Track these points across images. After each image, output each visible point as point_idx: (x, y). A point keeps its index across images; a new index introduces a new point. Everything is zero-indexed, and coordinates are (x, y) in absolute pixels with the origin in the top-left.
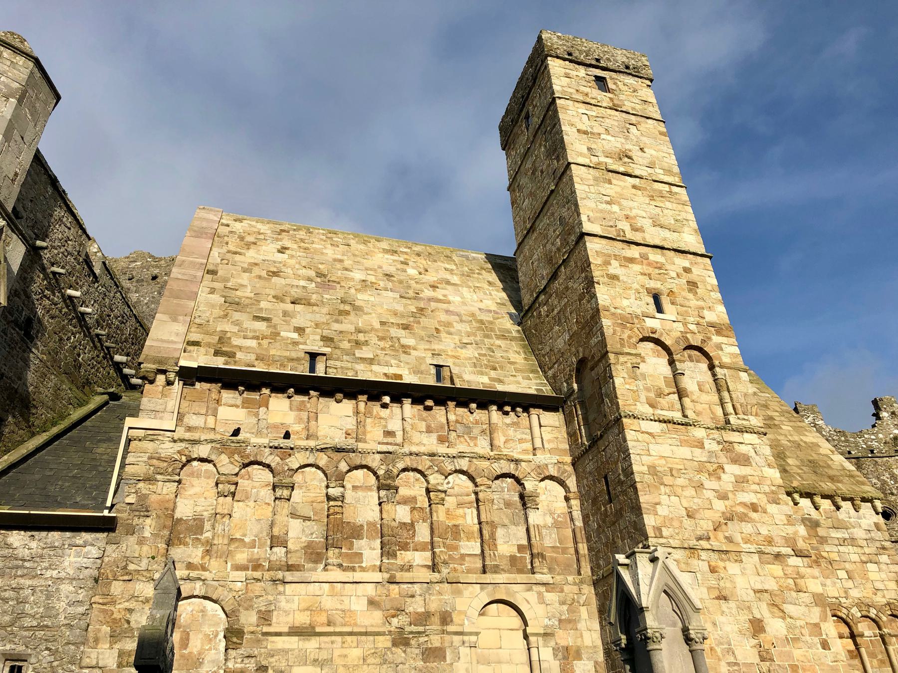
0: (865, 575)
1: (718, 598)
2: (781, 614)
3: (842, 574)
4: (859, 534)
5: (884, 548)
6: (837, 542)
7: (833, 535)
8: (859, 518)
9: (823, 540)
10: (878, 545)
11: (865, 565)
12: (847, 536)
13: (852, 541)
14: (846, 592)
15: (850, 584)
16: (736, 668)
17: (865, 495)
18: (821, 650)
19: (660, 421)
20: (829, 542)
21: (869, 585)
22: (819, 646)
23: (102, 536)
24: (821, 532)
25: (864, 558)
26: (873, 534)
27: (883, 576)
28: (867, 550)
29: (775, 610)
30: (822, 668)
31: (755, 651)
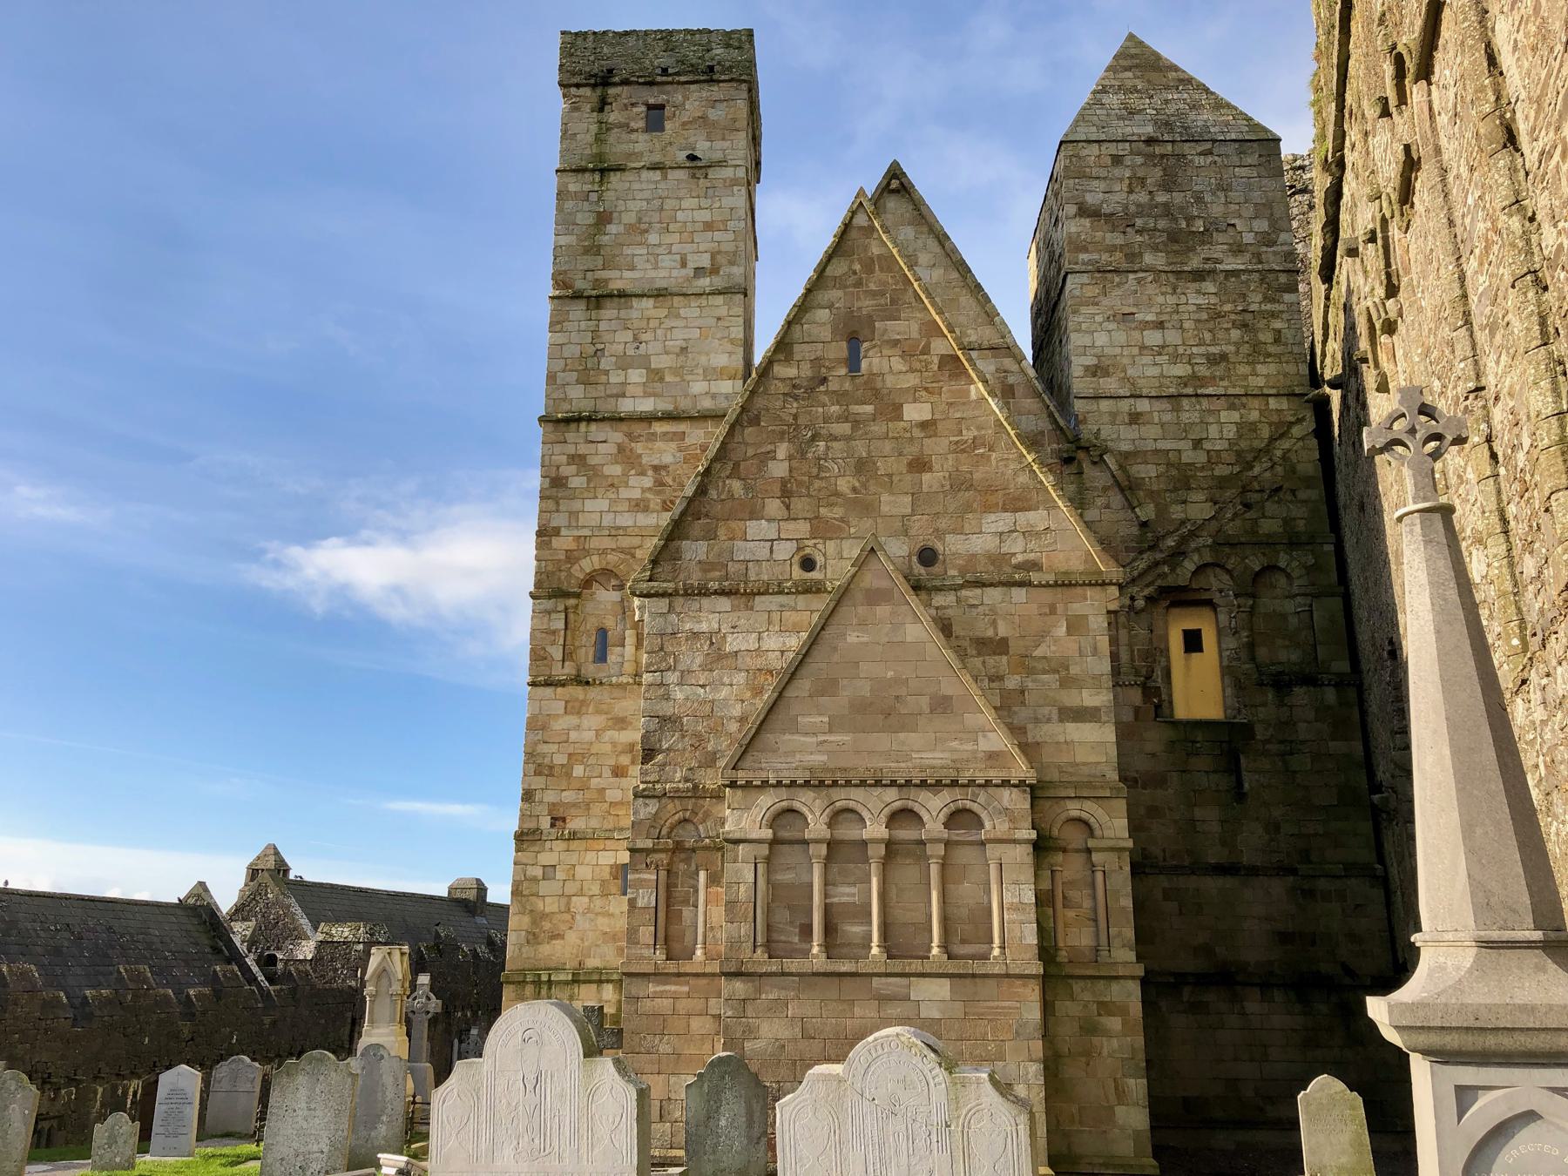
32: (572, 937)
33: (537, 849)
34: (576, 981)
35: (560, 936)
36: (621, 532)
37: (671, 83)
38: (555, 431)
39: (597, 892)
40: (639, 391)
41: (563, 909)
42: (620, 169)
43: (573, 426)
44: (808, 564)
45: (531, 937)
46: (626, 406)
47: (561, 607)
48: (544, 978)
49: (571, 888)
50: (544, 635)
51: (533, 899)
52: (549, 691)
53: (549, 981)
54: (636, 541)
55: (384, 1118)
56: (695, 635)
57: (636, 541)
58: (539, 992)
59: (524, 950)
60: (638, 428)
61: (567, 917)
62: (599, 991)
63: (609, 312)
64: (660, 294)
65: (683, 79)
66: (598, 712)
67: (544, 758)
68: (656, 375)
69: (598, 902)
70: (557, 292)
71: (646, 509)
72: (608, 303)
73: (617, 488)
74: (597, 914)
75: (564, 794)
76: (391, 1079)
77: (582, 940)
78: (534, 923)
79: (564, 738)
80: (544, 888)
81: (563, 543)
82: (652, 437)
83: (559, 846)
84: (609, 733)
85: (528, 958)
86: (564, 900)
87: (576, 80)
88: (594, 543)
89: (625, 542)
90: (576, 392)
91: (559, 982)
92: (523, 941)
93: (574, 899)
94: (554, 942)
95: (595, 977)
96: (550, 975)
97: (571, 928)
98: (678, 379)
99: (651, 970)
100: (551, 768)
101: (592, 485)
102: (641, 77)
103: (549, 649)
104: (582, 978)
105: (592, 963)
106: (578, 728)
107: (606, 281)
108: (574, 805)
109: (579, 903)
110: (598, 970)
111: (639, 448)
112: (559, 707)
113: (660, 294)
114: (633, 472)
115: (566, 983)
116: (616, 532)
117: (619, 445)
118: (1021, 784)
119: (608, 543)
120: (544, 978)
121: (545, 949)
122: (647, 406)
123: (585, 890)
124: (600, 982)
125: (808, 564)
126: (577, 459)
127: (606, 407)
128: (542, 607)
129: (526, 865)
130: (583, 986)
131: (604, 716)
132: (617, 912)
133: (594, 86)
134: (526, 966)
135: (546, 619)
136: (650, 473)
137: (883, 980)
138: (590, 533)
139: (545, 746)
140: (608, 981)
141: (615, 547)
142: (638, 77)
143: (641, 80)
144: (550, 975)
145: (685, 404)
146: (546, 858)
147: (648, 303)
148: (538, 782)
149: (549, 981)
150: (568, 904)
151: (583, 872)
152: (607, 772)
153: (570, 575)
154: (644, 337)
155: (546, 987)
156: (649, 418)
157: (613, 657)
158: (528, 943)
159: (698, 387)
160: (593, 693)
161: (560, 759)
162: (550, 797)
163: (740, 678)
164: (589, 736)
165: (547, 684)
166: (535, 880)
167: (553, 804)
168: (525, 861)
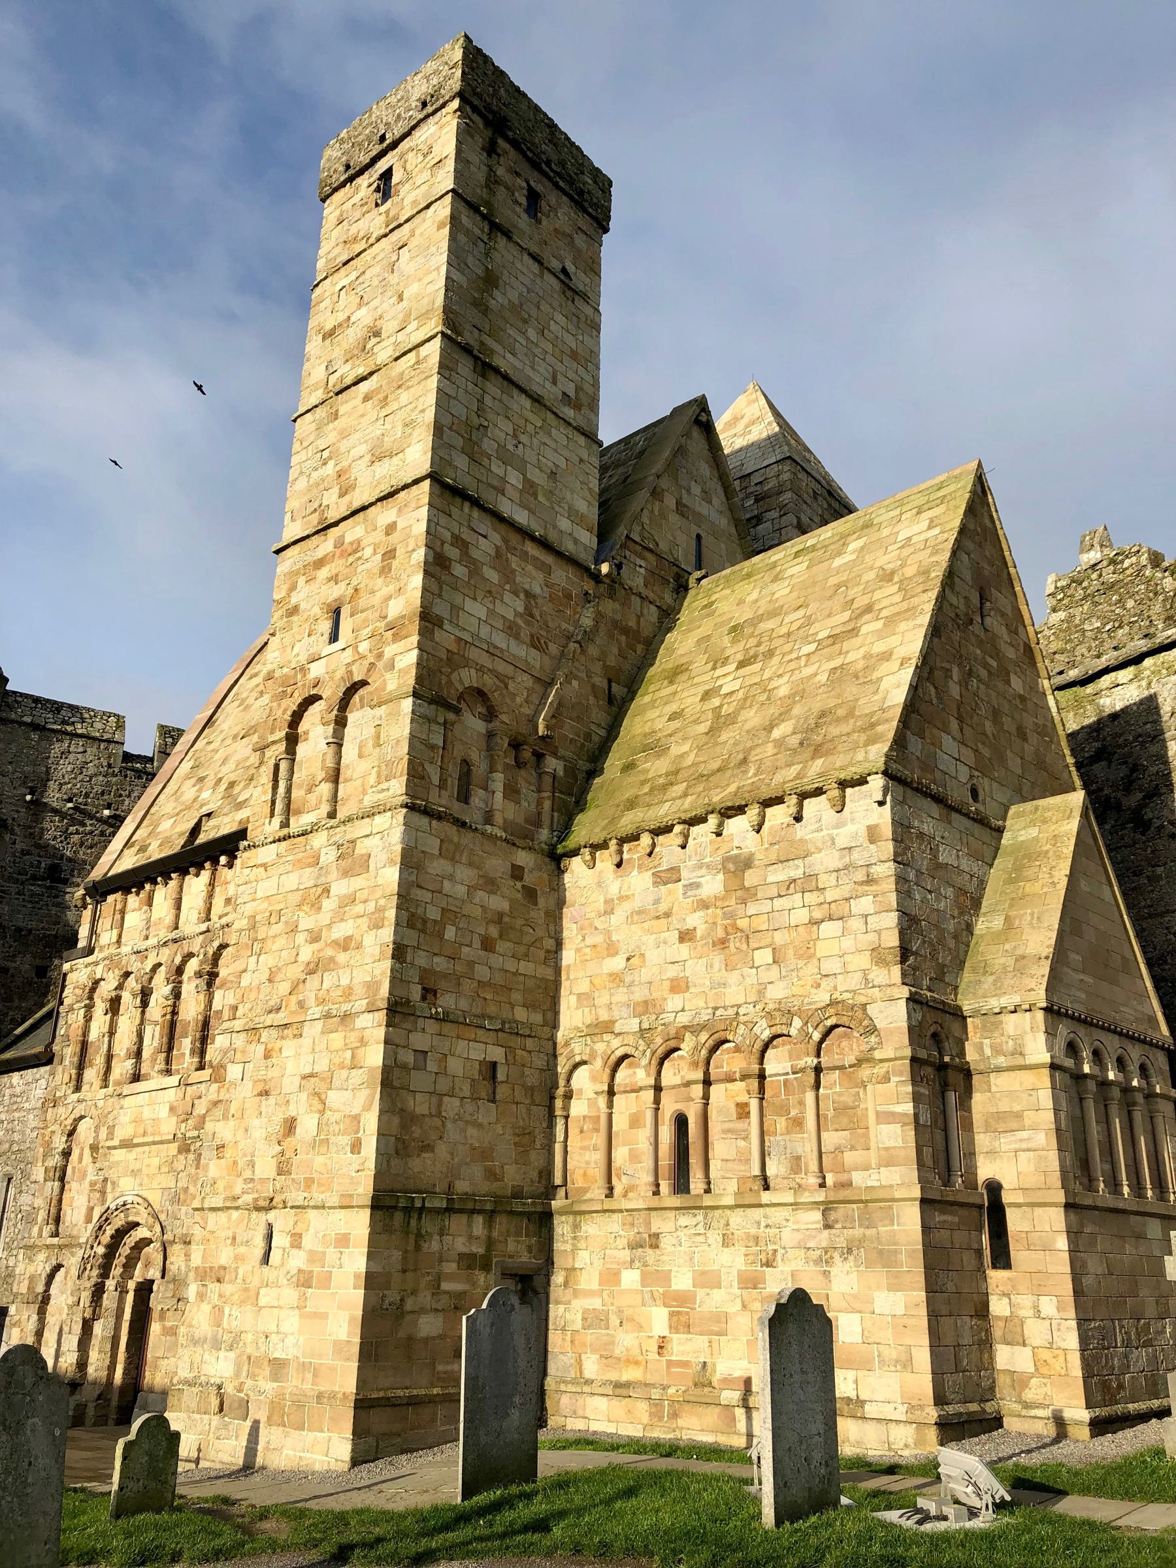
0: (807, 953)
1: (260, 1094)
2: (320, 1107)
3: (763, 957)
4: (825, 861)
5: (870, 881)
6: (774, 892)
7: (770, 879)
8: (838, 826)
9: (748, 895)
10: (860, 876)
11: (815, 927)
12: (798, 873)
13: (808, 883)
14: (759, 992)
15: (774, 973)
16: (250, 1185)
17: (842, 776)
18: (349, 1155)
19: (279, 840)
20: (759, 896)
21: (811, 969)
22: (348, 1149)
23: (43, 1069)
24: (751, 878)
25: (818, 915)
26: (855, 855)
27: (848, 943)
28: (830, 895)
29: (316, 1102)
30: (341, 1181)
31: (274, 1162)
32: (442, 1150)
33: (408, 1025)
34: (449, 1210)
35: (428, 1148)
36: (497, 653)
37: (550, 179)
38: (440, 496)
39: (467, 1093)
40: (516, 496)
41: (434, 1112)
42: (508, 235)
43: (458, 500)
44: (974, 793)
45: (400, 1146)
46: (506, 508)
47: (441, 720)
48: (418, 1204)
49: (443, 1085)
50: (423, 747)
51: (403, 1092)
52: (424, 821)
53: (423, 1208)
54: (510, 670)
55: (517, 1399)
56: (921, 835)
57: (510, 670)
58: (409, 1223)
59: (392, 1163)
60: (514, 539)
61: (437, 1122)
62: (470, 1225)
63: (493, 388)
64: (537, 400)
65: (562, 184)
66: (470, 864)
67: (417, 906)
68: (530, 488)
69: (469, 1107)
70: (449, 332)
71: (517, 637)
72: (492, 375)
73: (495, 598)
74: (467, 1122)
75: (436, 959)
76: (523, 1340)
77: (452, 1154)
78: (404, 1126)
79: (436, 887)
80: (419, 1081)
81: (445, 638)
82: (524, 556)
83: (432, 1026)
84: (480, 893)
85: (397, 1175)
86: (434, 1100)
87: (476, 102)
88: (474, 654)
89: (502, 667)
90: (461, 462)
91: (430, 1210)
92: (392, 1152)
93: (446, 1099)
94: (424, 1155)
95: (470, 1206)
96: (424, 1199)
97: (441, 1138)
98: (547, 504)
99: (939, 1198)
100: (425, 921)
101: (472, 582)
102: (531, 151)
103: (427, 765)
104: (456, 1206)
105: (462, 1186)
106: (451, 878)
107: (492, 352)
108: (446, 976)
109: (451, 1106)
110: (467, 1197)
111: (514, 562)
112: (432, 845)
113: (537, 400)
114: (507, 587)
115: (437, 1211)
116: (492, 652)
117: (497, 547)
118: (1168, 1050)
119: (484, 659)
120: (418, 1204)
121: (415, 1164)
122: (521, 517)
123: (457, 1090)
124: (473, 1212)
125: (974, 793)
126: (458, 541)
127: (488, 497)
128: (422, 710)
129: (397, 1046)
130: (454, 1217)
131: (476, 871)
132: (485, 1122)
133: (487, 123)
134: (397, 1186)
135: (426, 726)
136: (522, 596)
137: (1138, 1218)
138: (470, 640)
139: (419, 892)
140: (479, 1212)
141: (490, 667)
142: (528, 149)
143: (530, 154)
144: (424, 1199)
145: (552, 537)
146: (420, 1041)
147: (527, 403)
148: (411, 937)
149: (423, 1208)
150: (440, 1105)
151: (455, 1066)
152: (477, 944)
153: (450, 682)
154: (524, 438)
155: (416, 1216)
156: (526, 534)
157: (478, 798)
158: (397, 1153)
159: (564, 524)
160: (467, 838)
161: (433, 914)
162: (421, 959)
163: (950, 892)
164: (461, 890)
165: (426, 812)
166: (404, 1067)
167: (425, 969)
168: (397, 1041)
